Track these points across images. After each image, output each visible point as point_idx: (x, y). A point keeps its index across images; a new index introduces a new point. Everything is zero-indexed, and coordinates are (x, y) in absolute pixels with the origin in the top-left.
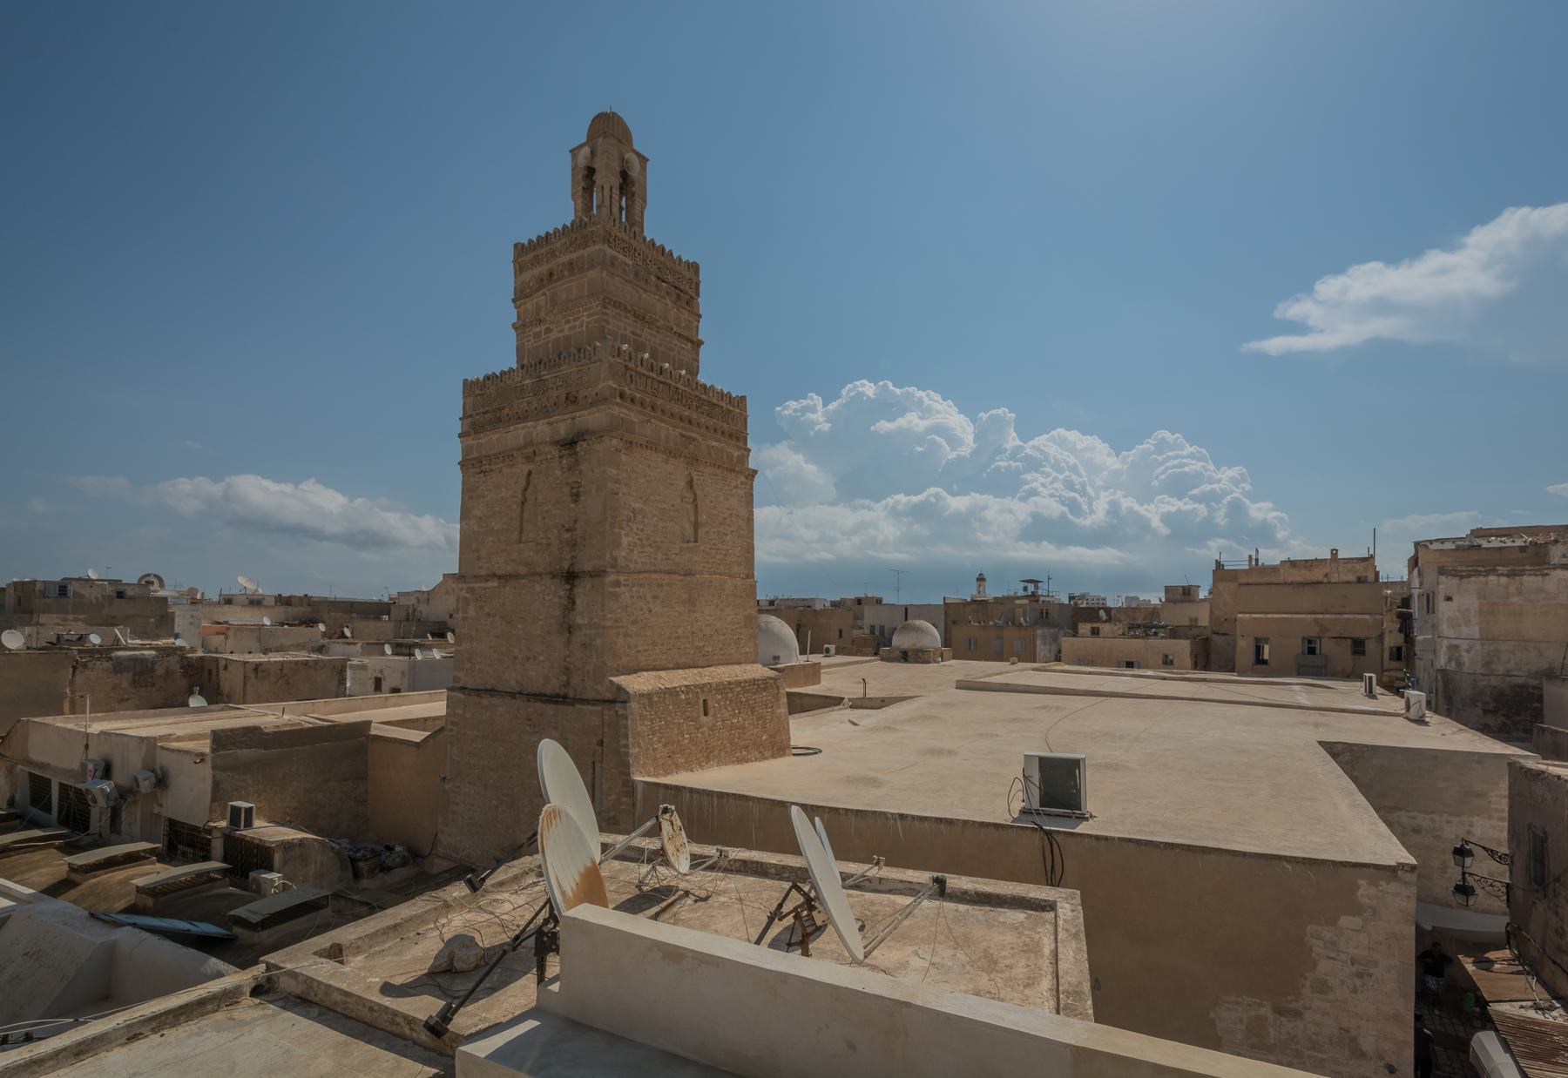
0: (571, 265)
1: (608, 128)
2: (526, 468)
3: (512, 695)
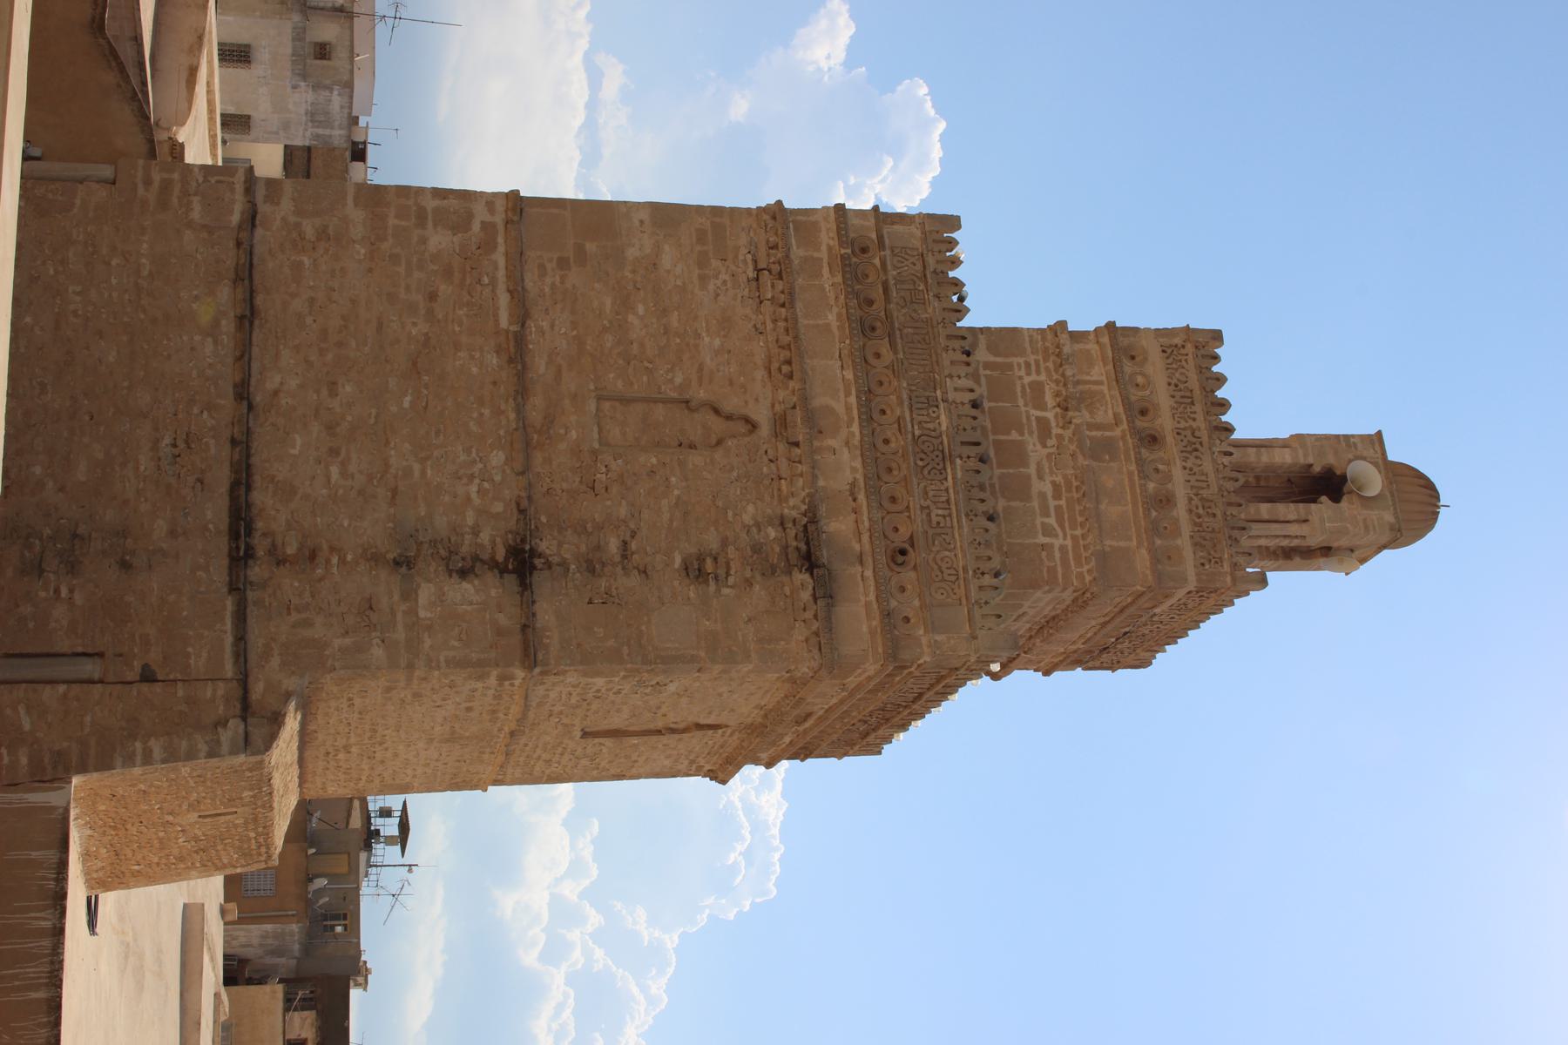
0: (1165, 501)
1: (1412, 505)
2: (762, 415)
3: (242, 392)
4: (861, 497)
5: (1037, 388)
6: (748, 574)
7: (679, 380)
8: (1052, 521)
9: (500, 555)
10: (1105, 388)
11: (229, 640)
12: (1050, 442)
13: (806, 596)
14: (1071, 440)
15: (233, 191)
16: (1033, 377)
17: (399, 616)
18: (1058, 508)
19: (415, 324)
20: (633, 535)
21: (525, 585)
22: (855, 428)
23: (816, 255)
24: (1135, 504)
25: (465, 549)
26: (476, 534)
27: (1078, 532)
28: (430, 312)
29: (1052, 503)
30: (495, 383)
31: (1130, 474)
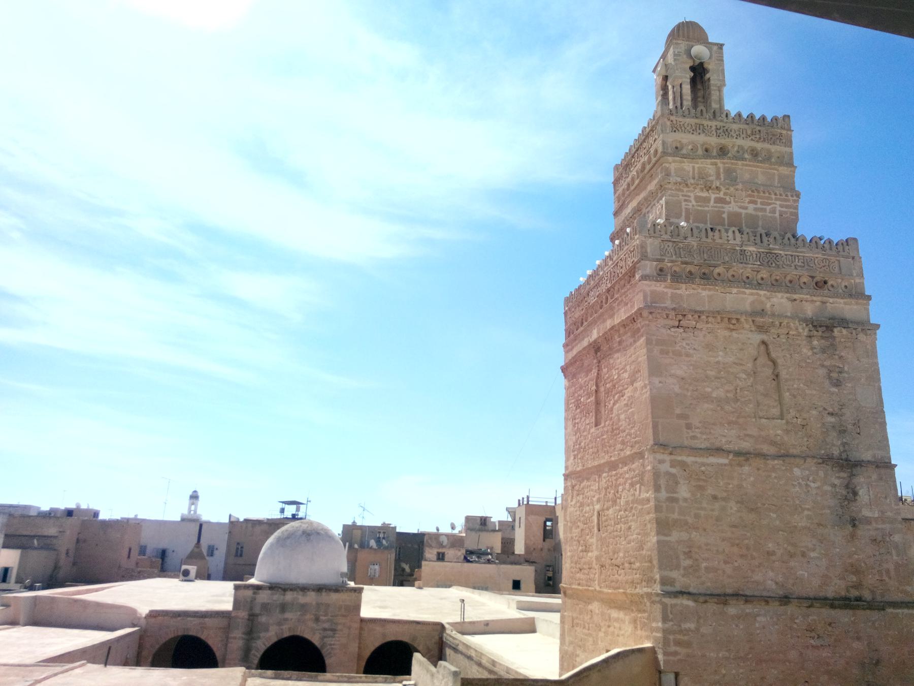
3: (785, 600)
4: (796, 296)
5: (698, 199)
6: (837, 357)
7: (744, 376)
8: (768, 208)
10: (697, 166)
11: (906, 611)
12: (728, 199)
13: (845, 331)
14: (728, 189)
15: (676, 605)
16: (692, 199)
17: (880, 526)
18: (762, 203)
19: (731, 508)
20: (825, 409)
21: (858, 464)
22: (762, 293)
23: (669, 295)
24: (758, 167)
25: (844, 493)
26: (834, 486)
27: (773, 197)
28: (724, 499)
29: (759, 206)
30: (758, 469)
31: (743, 165)
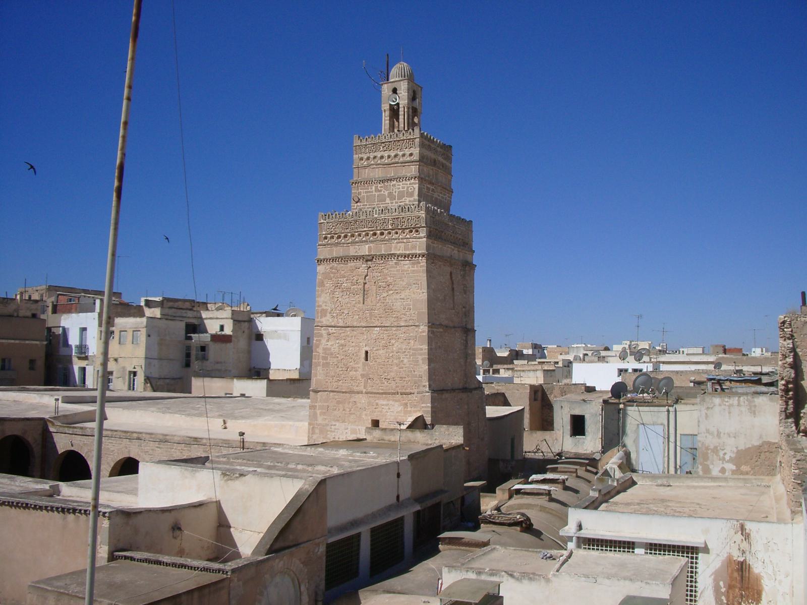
9: (465, 335)
16: (425, 187)
26: (463, 340)
